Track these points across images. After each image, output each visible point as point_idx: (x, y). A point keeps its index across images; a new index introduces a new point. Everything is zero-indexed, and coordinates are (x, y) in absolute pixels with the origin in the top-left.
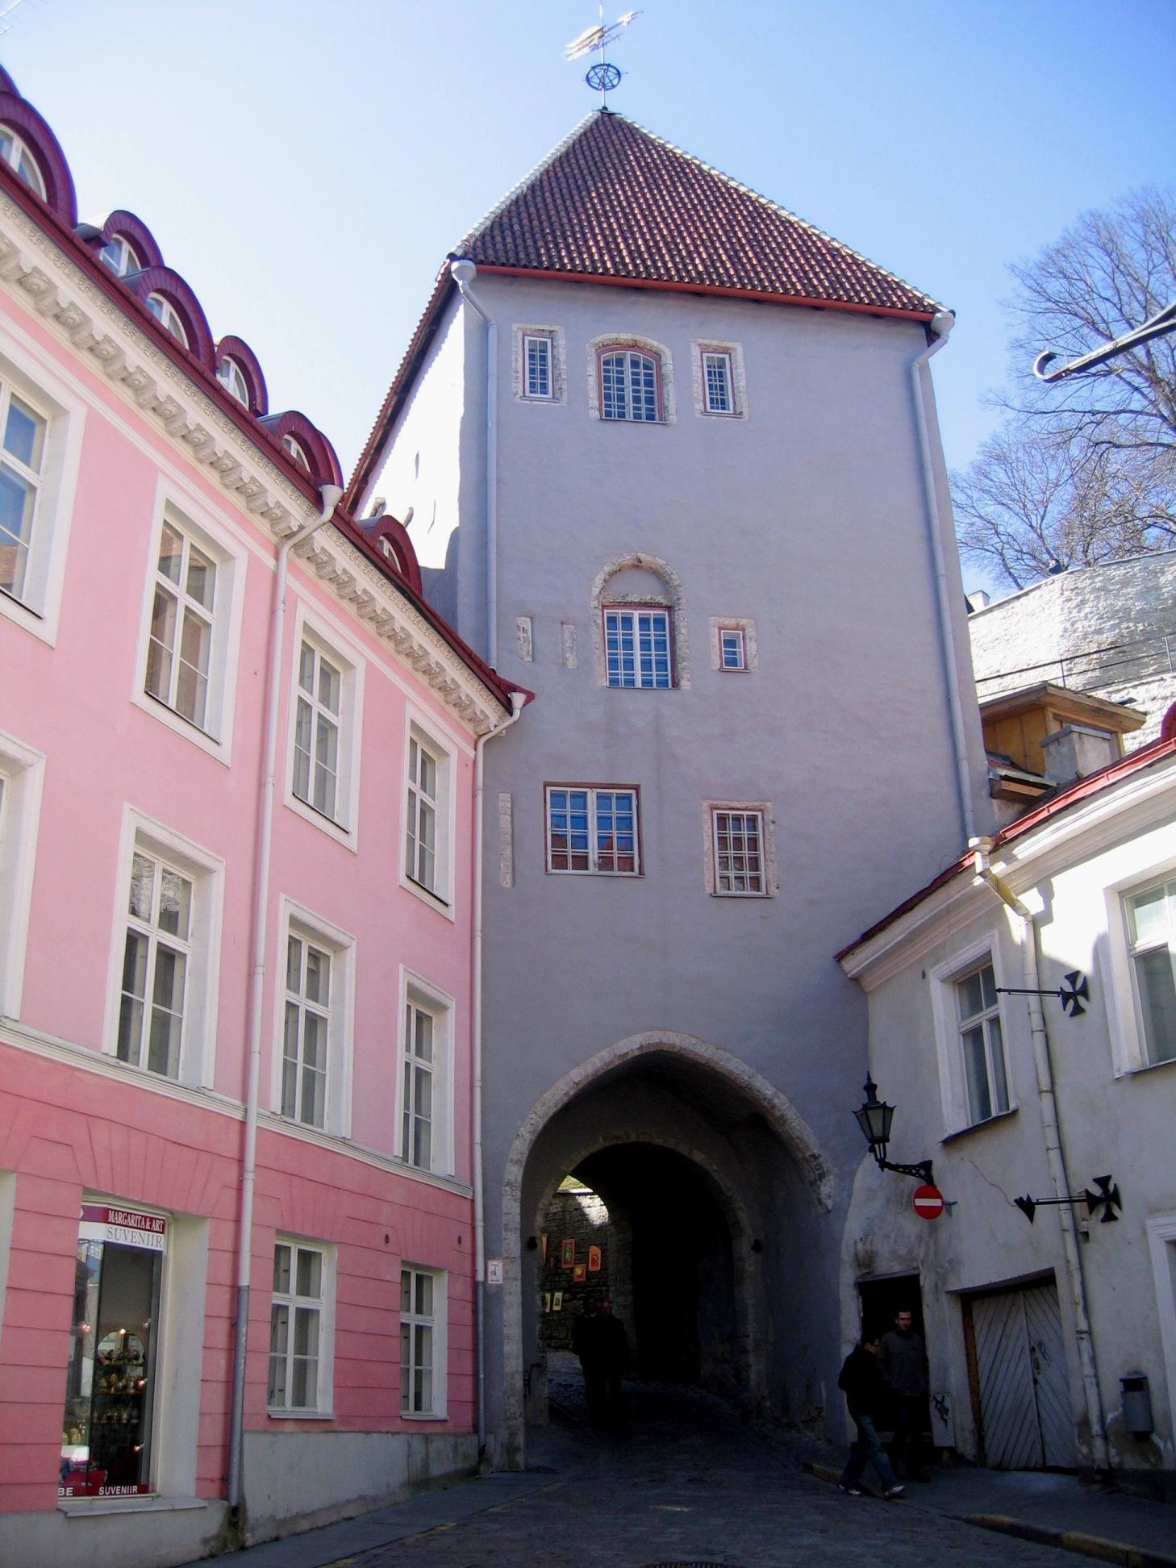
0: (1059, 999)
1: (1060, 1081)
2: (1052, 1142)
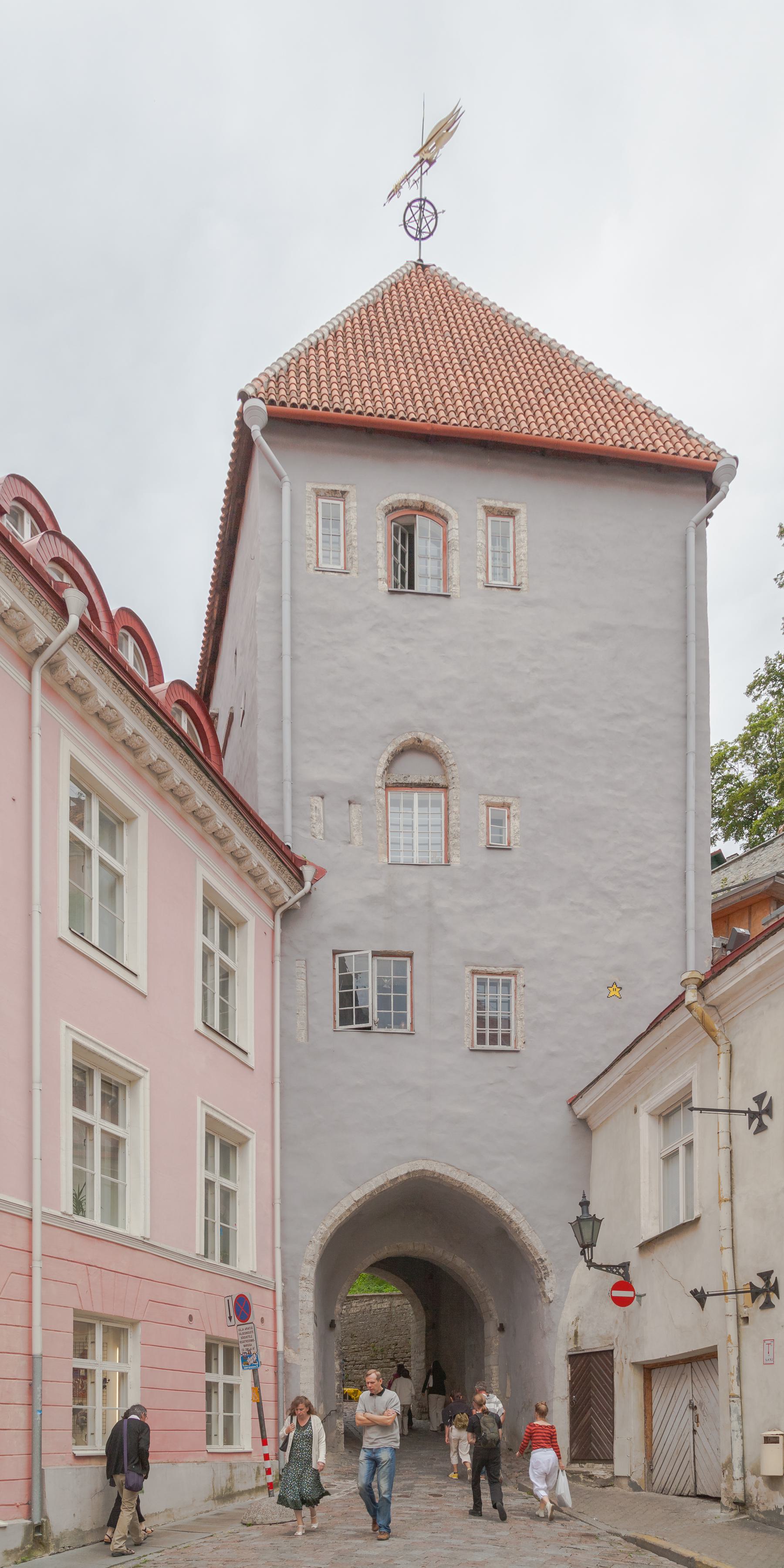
1: (737, 1191)
2: (726, 1242)
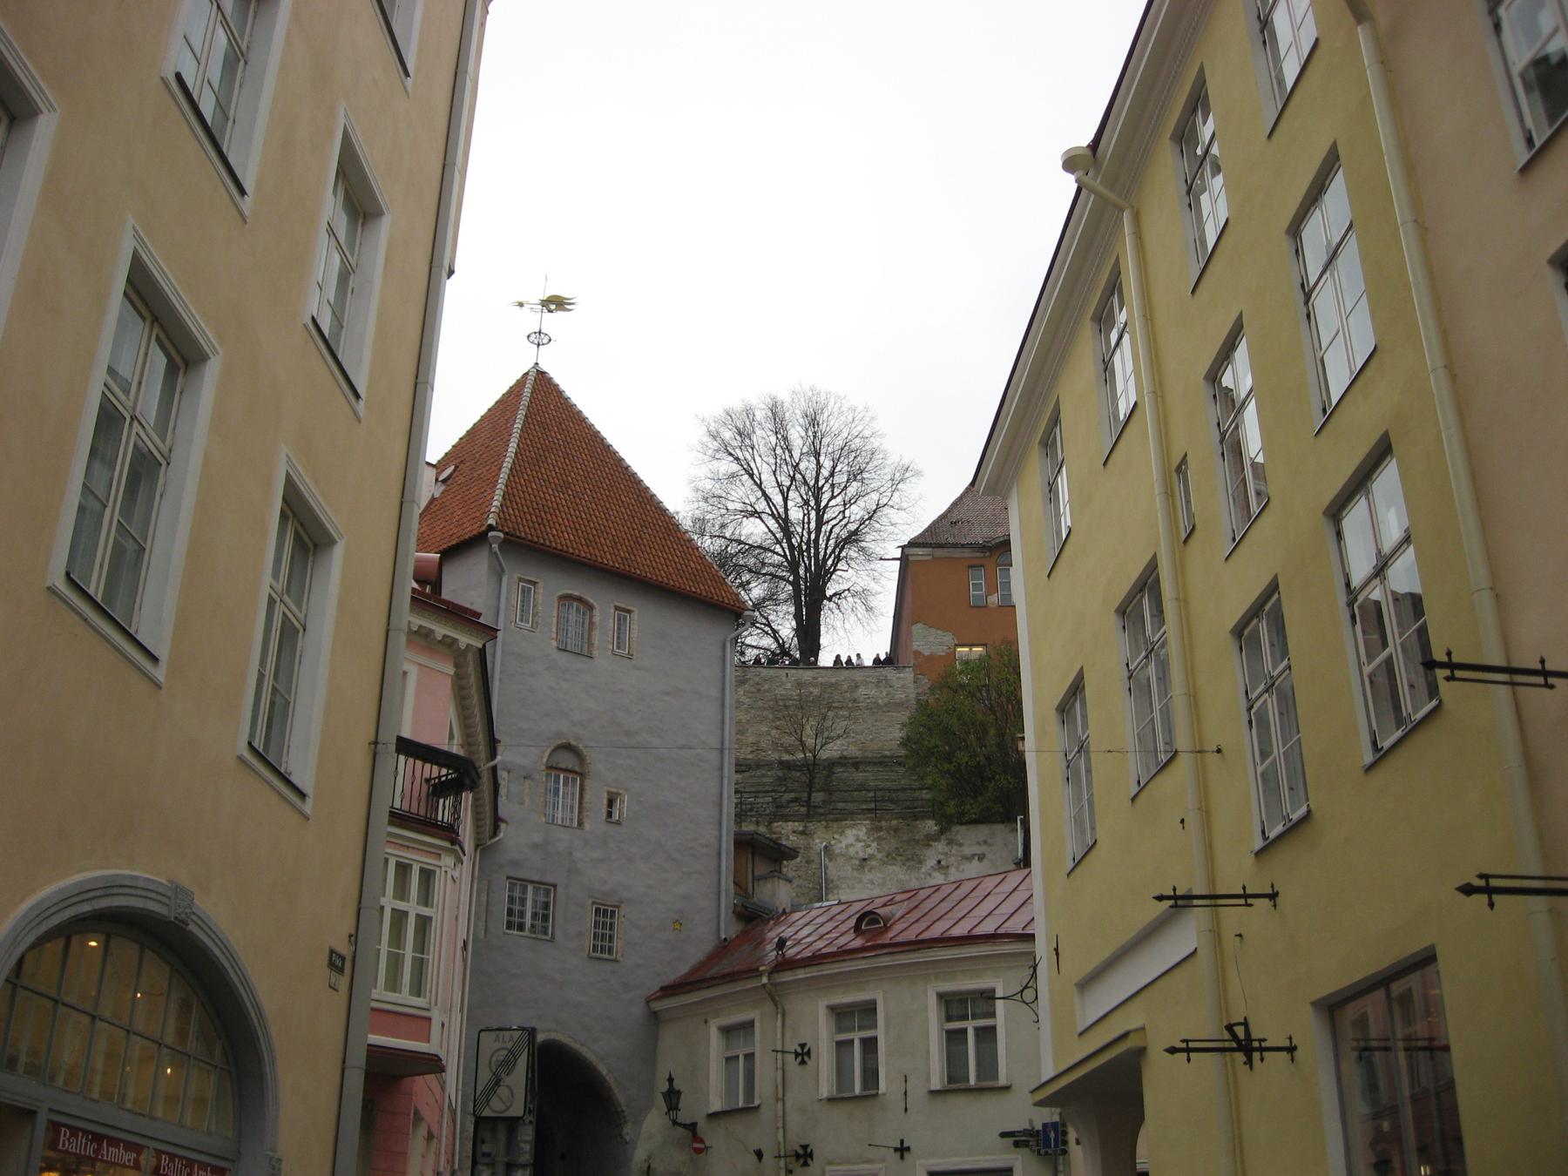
1: (788, 1095)
2: (780, 1124)
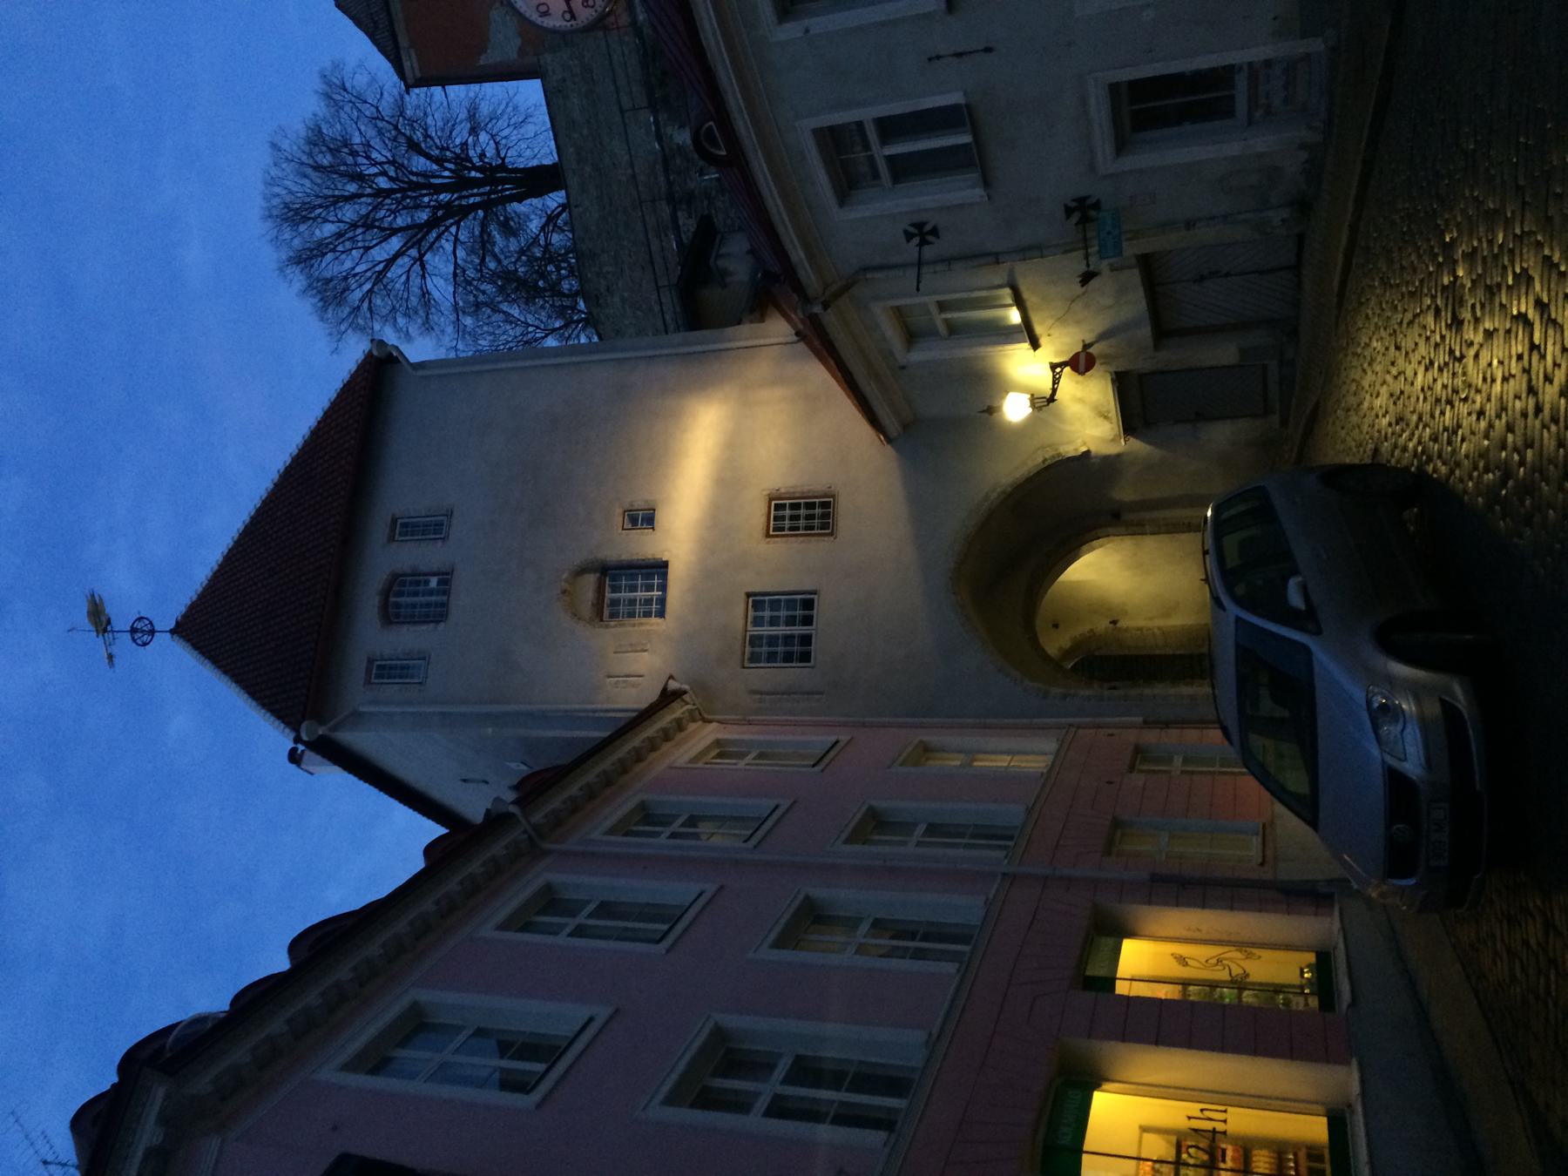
0: (926, 248)
